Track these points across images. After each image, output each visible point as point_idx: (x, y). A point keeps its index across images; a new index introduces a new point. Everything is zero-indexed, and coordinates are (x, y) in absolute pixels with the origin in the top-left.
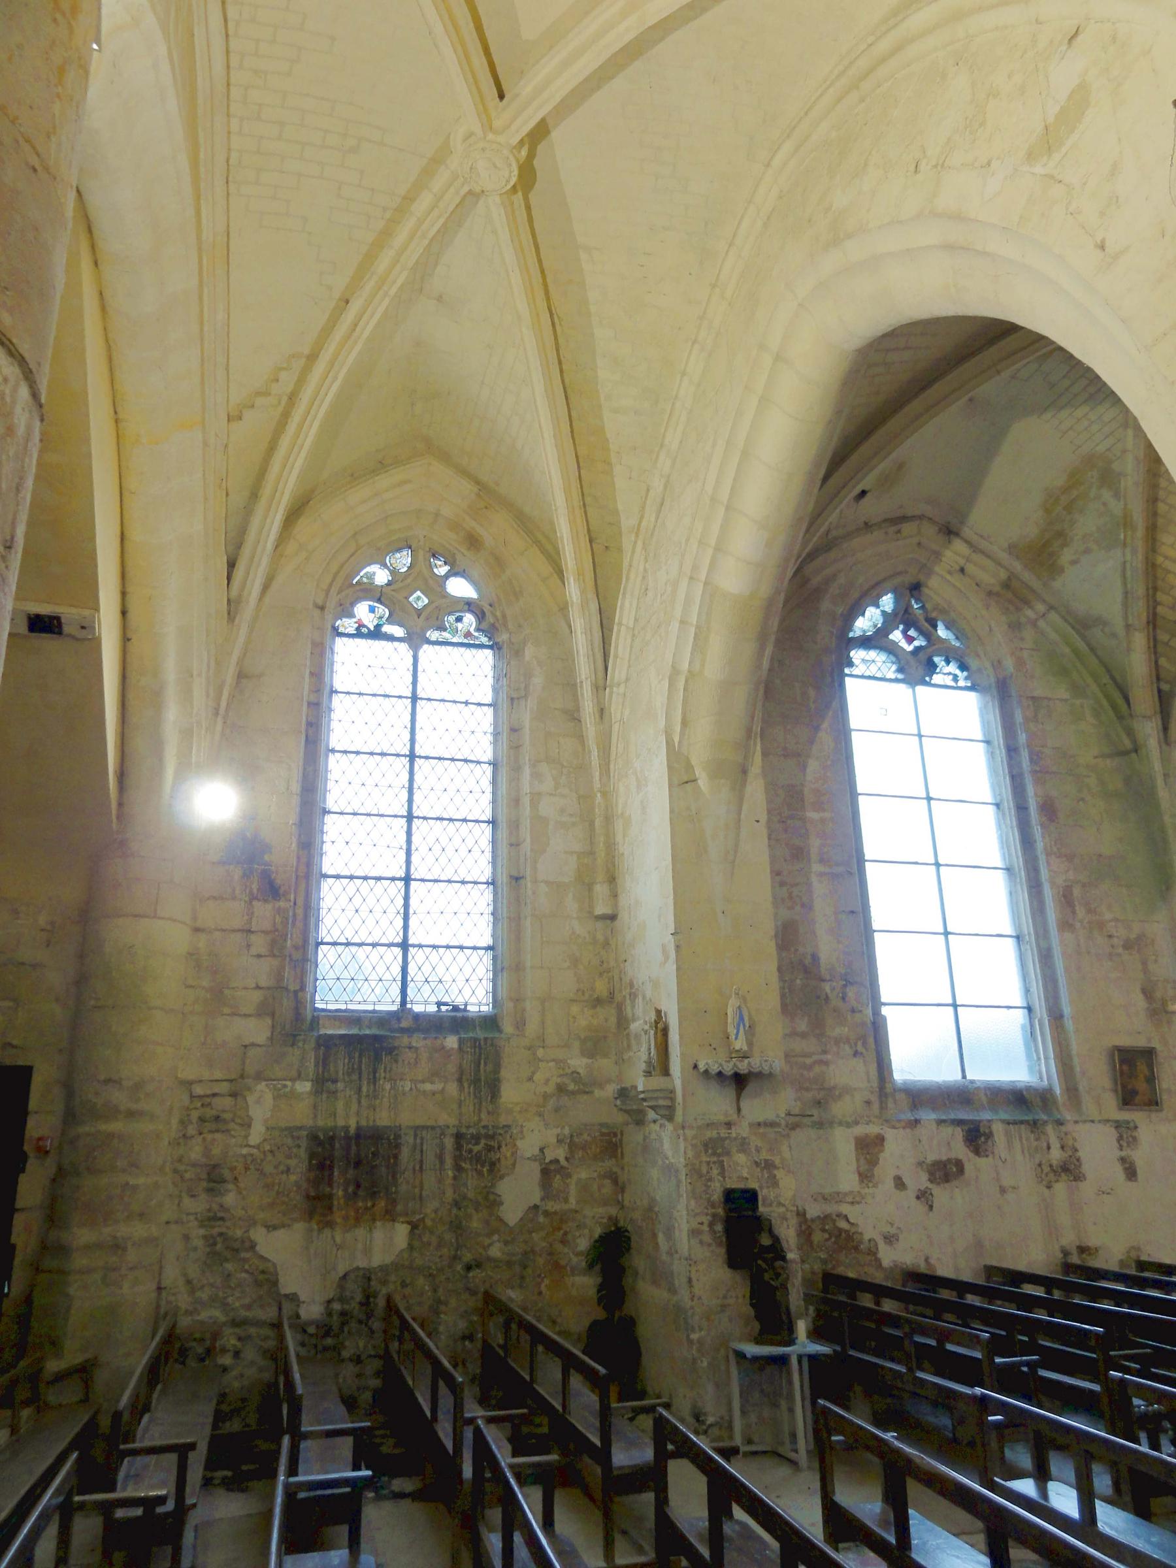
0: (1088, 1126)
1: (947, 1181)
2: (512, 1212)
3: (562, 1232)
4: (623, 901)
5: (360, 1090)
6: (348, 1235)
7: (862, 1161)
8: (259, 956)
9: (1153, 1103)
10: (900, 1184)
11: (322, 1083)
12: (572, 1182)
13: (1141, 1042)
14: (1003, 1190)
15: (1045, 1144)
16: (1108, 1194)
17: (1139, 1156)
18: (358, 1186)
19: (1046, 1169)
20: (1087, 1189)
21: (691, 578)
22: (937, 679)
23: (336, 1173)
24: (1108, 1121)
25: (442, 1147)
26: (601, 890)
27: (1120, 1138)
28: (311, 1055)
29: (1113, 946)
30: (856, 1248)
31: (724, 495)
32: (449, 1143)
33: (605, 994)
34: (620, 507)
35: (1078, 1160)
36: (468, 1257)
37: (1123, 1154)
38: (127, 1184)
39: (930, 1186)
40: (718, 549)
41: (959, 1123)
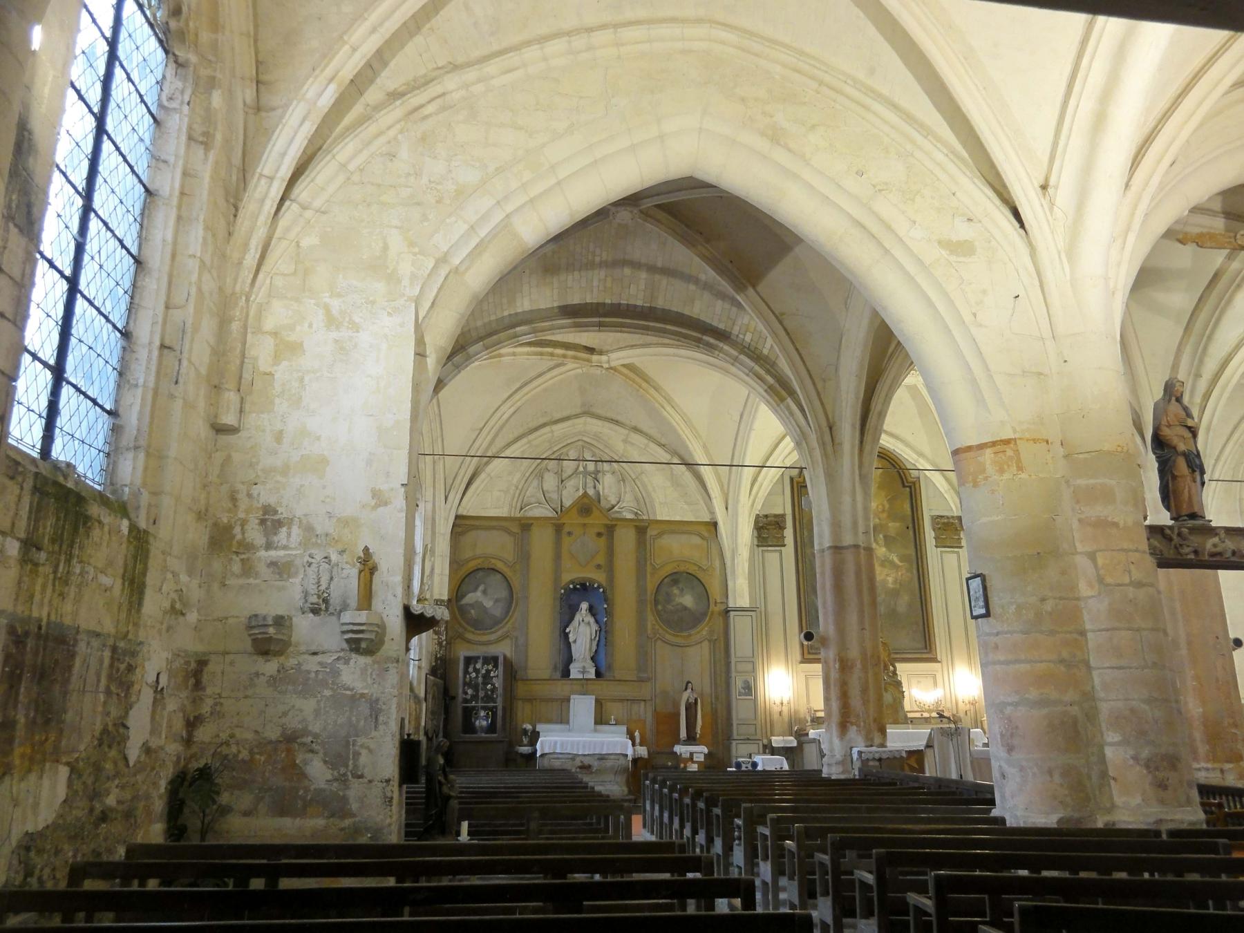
2: (133, 753)
3: (155, 772)
4: (251, 419)
5: (57, 567)
6: (23, 785)
11: (30, 544)
12: (165, 713)
18: (36, 710)
21: (498, 202)
23: (22, 690)
25: (101, 661)
26: (231, 397)
28: (26, 500)
31: (562, 174)
32: (107, 654)
33: (203, 509)
34: (392, 64)
36: (98, 807)
40: (532, 201)
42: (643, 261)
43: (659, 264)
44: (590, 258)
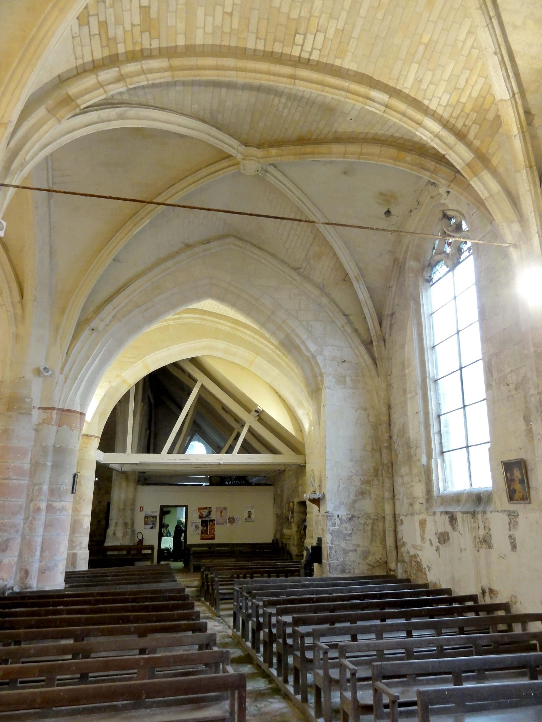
0: (497, 513)
1: (445, 543)
7: (421, 531)
9: (526, 498)
10: (431, 544)
13: (521, 455)
14: (461, 551)
15: (477, 525)
16: (503, 558)
17: (518, 534)
19: (478, 540)
20: (494, 553)
22: (463, 257)
24: (505, 511)
27: (510, 521)
29: (510, 391)
30: (422, 570)
35: (491, 536)
37: (511, 533)
39: (439, 545)
41: (447, 513)
42: (240, 92)
43: (224, 90)
44: (289, 104)
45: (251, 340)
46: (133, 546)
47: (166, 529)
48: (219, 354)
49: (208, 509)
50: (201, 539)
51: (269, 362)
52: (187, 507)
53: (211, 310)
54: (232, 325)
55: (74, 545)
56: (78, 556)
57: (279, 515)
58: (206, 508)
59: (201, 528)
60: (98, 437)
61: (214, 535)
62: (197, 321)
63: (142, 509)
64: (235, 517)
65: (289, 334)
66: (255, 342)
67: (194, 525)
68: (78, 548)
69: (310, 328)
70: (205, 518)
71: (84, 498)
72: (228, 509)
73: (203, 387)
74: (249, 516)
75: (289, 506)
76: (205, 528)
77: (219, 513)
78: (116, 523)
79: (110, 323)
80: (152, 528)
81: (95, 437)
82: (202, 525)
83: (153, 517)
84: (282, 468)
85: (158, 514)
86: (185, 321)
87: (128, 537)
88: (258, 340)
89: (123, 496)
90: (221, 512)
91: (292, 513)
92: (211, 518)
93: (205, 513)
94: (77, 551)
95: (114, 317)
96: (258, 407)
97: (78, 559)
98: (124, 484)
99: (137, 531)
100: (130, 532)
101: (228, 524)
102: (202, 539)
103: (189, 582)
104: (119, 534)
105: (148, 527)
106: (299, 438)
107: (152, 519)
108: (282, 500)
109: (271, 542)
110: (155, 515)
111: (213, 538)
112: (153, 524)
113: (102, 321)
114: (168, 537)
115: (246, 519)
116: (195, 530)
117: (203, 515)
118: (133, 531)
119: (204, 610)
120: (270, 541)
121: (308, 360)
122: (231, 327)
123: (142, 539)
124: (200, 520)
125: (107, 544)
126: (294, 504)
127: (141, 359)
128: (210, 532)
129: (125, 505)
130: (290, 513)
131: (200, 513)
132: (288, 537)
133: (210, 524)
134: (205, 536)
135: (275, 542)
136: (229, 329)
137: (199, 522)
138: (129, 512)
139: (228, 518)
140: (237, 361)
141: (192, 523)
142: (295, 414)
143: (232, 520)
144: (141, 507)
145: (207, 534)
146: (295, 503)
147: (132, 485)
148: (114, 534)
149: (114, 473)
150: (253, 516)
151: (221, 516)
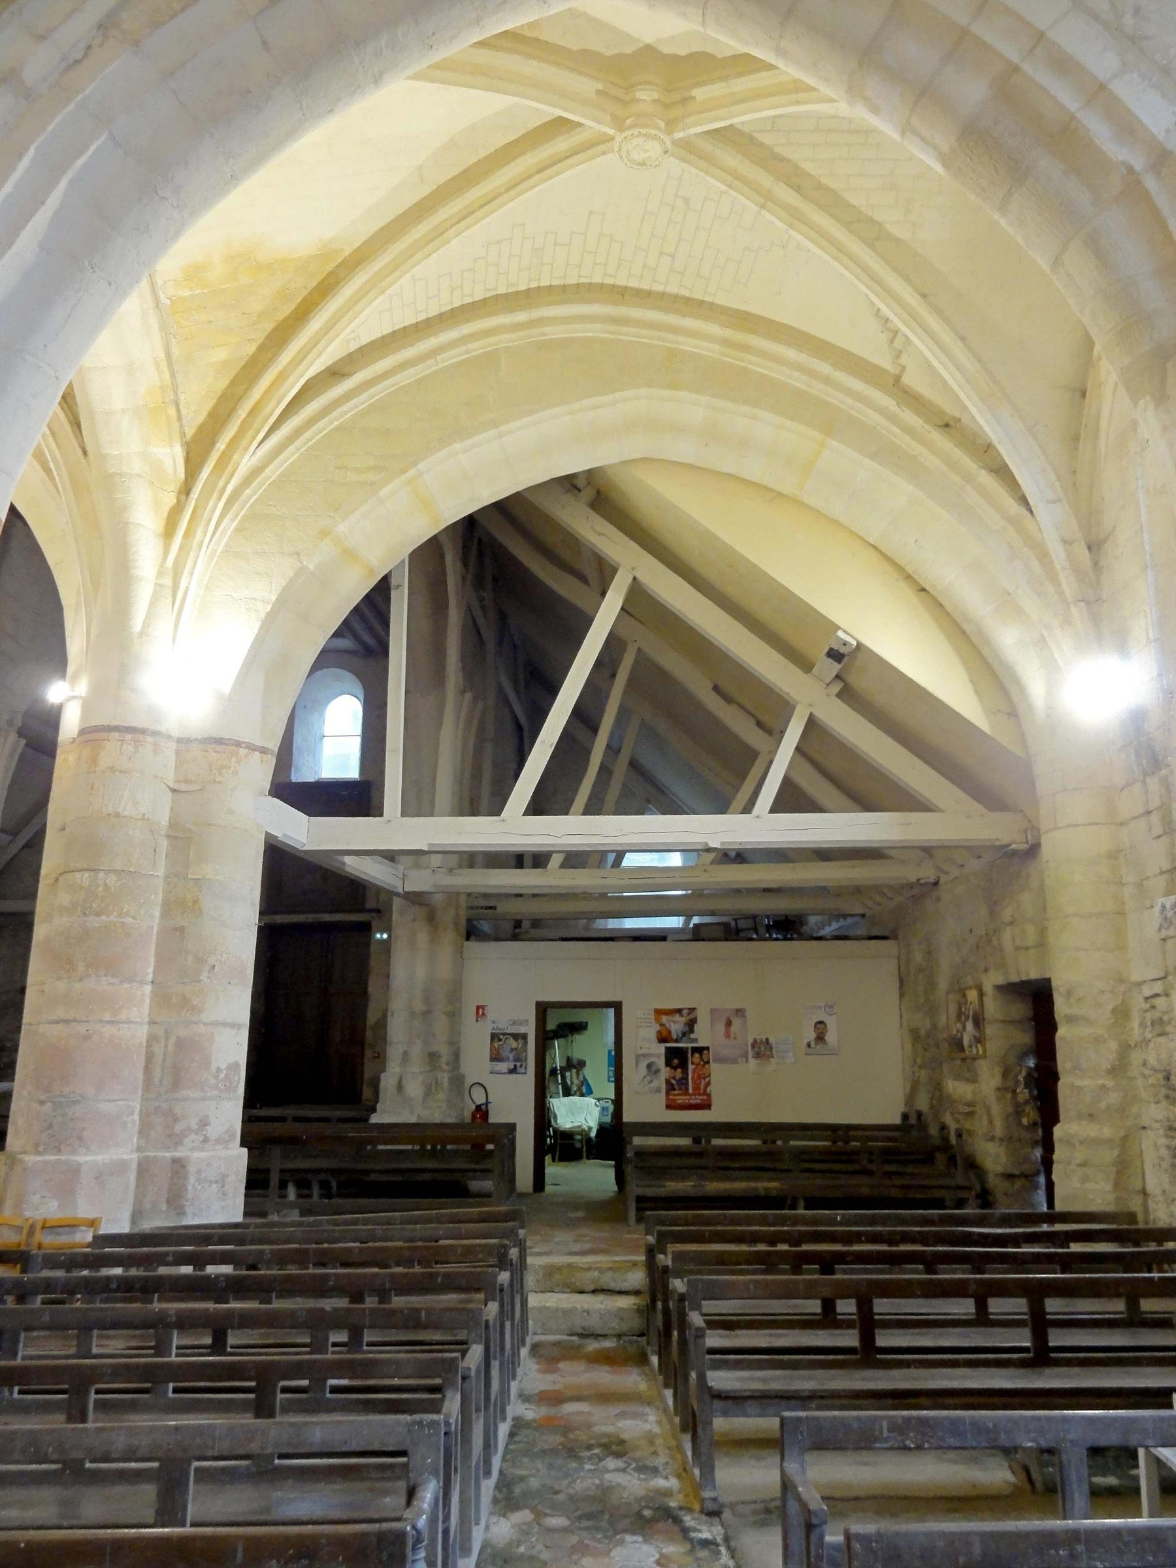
8: (1159, 837)
38: (1073, 1085)
45: (799, 381)
46: (460, 1126)
47: (578, 1074)
48: (685, 450)
49: (685, 1012)
50: (668, 1107)
51: (874, 456)
52: (617, 1006)
53: (645, 285)
54: (729, 333)
55: (178, 1128)
56: (192, 1169)
57: (923, 1032)
58: (679, 1011)
59: (665, 1072)
60: (264, 751)
61: (709, 1095)
62: (594, 331)
63: (481, 1012)
64: (772, 1040)
65: (1016, 69)
66: (817, 389)
67: (643, 1064)
68: (191, 1139)
69: (1128, 20)
70: (677, 1041)
71: (212, 960)
72: (748, 1014)
73: (636, 591)
74: (820, 1038)
75: (962, 1003)
76: (679, 1073)
77: (721, 1027)
78: (405, 1053)
79: (86, 56)
80: (513, 1071)
81: (252, 748)
82: (668, 1063)
83: (516, 1036)
84: (927, 873)
85: (530, 1030)
86: (555, 332)
87: (441, 1096)
88: (827, 381)
89: (421, 971)
90: (729, 1024)
91: (978, 1022)
92: (695, 1040)
93: (676, 1026)
94: (195, 1155)
95: (103, 27)
96: (840, 634)
97: (192, 1179)
98: (423, 937)
99: (469, 1081)
100: (446, 1081)
101: (751, 1060)
102: (668, 1107)
103: (610, 1274)
104: (414, 1088)
105: (503, 1067)
106: (1005, 739)
107: (514, 1044)
108: (931, 985)
109: (897, 1120)
110: (522, 1030)
111: (706, 1106)
112: (517, 1059)
113: (42, 38)
114: (582, 1095)
115: (809, 1045)
116: (649, 1078)
117: (670, 1032)
118: (457, 1081)
119: (651, 1439)
120: (891, 1116)
121: (1132, 185)
122: (725, 342)
123: (487, 1103)
124: (661, 1049)
125: (375, 1119)
126: (981, 994)
127: (403, 471)
128: (696, 1087)
129: (427, 1000)
130: (970, 1026)
131: (662, 1025)
132: (968, 1109)
133: (693, 1061)
134: (681, 1099)
135: (912, 1123)
136: (716, 347)
137: (658, 1056)
138: (441, 1024)
139: (750, 1041)
140: (754, 469)
141: (638, 1058)
142: (986, 652)
143: (763, 1049)
144: (478, 1008)
145: (686, 1092)
146: (988, 988)
147: (449, 937)
148: (400, 1087)
149: (397, 903)
150: (831, 1037)
151: (727, 1035)
